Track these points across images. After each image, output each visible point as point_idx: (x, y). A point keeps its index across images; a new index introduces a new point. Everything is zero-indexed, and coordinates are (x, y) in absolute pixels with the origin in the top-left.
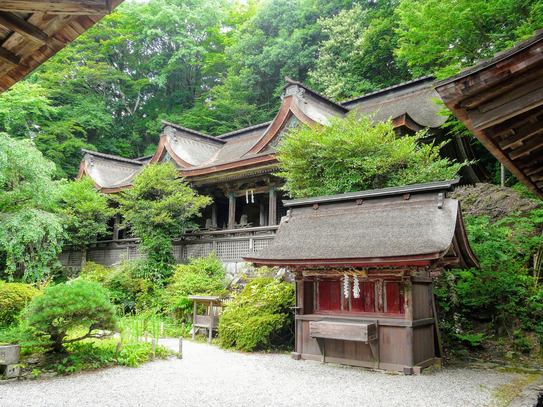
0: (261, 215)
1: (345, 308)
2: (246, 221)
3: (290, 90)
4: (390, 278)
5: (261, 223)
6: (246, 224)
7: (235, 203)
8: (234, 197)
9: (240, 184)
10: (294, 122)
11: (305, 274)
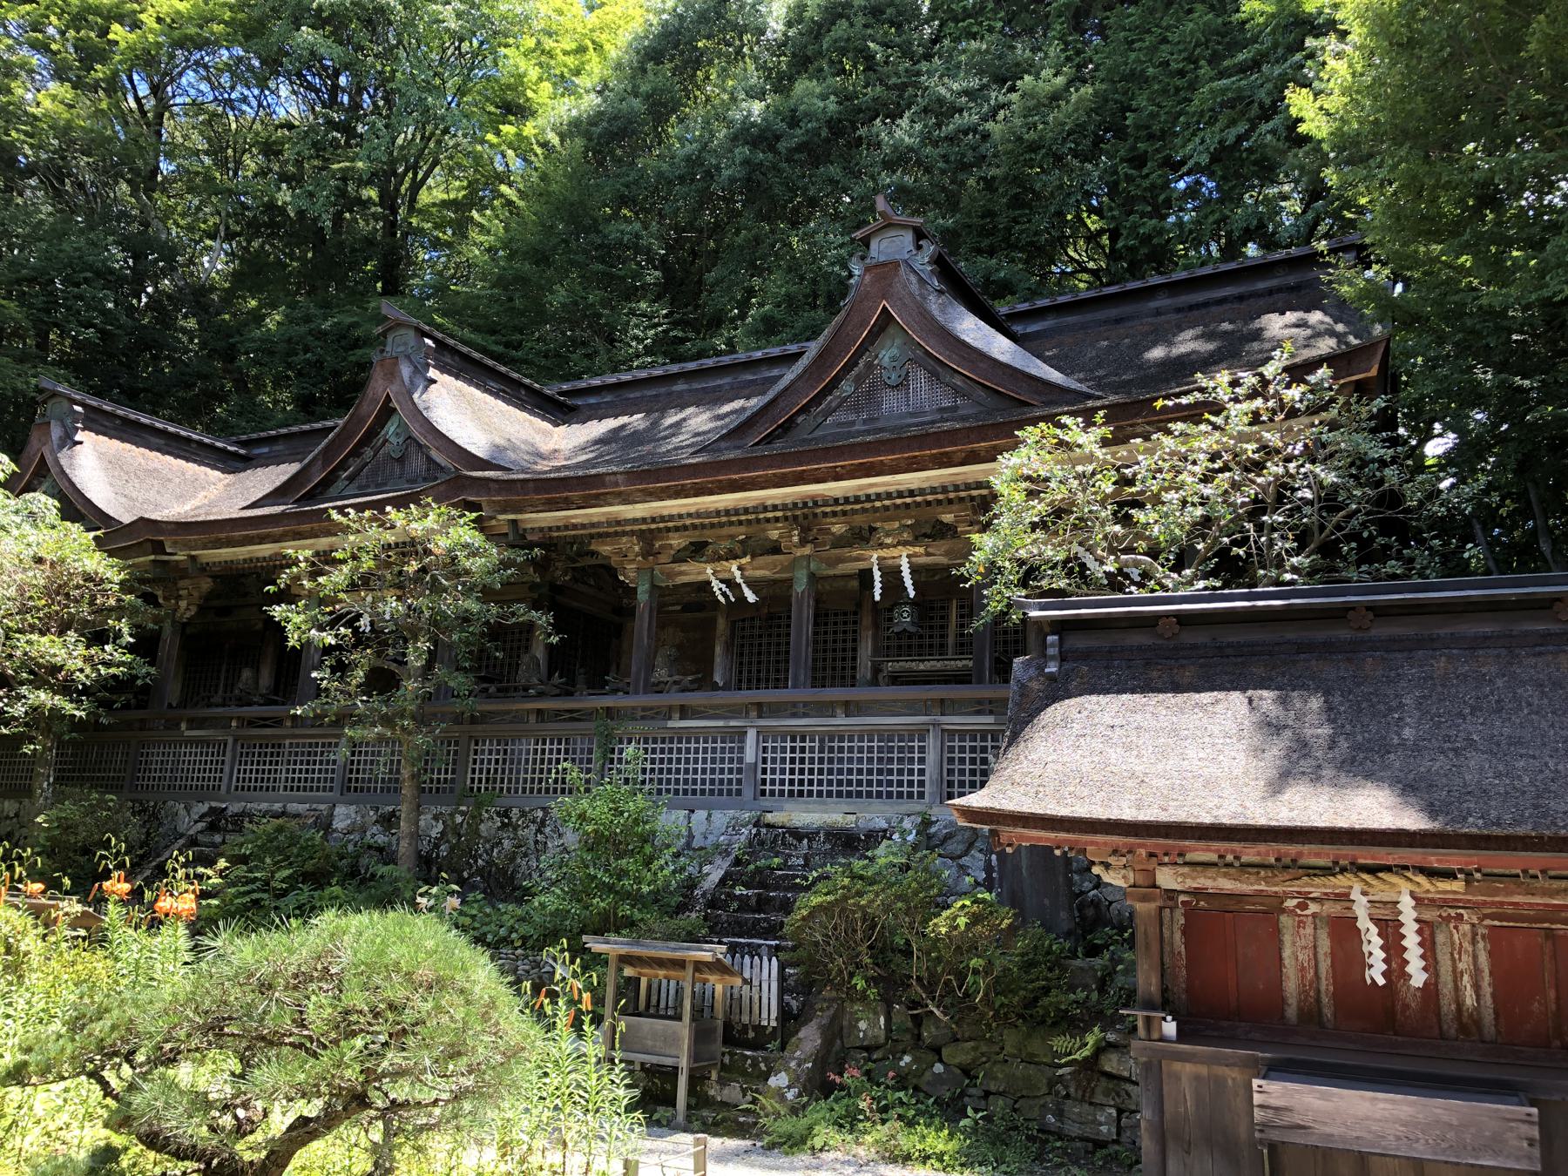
0: (718, 650)
3: (885, 243)
4: (1509, 910)
6: (676, 678)
8: (654, 587)
9: (677, 541)
10: (894, 351)
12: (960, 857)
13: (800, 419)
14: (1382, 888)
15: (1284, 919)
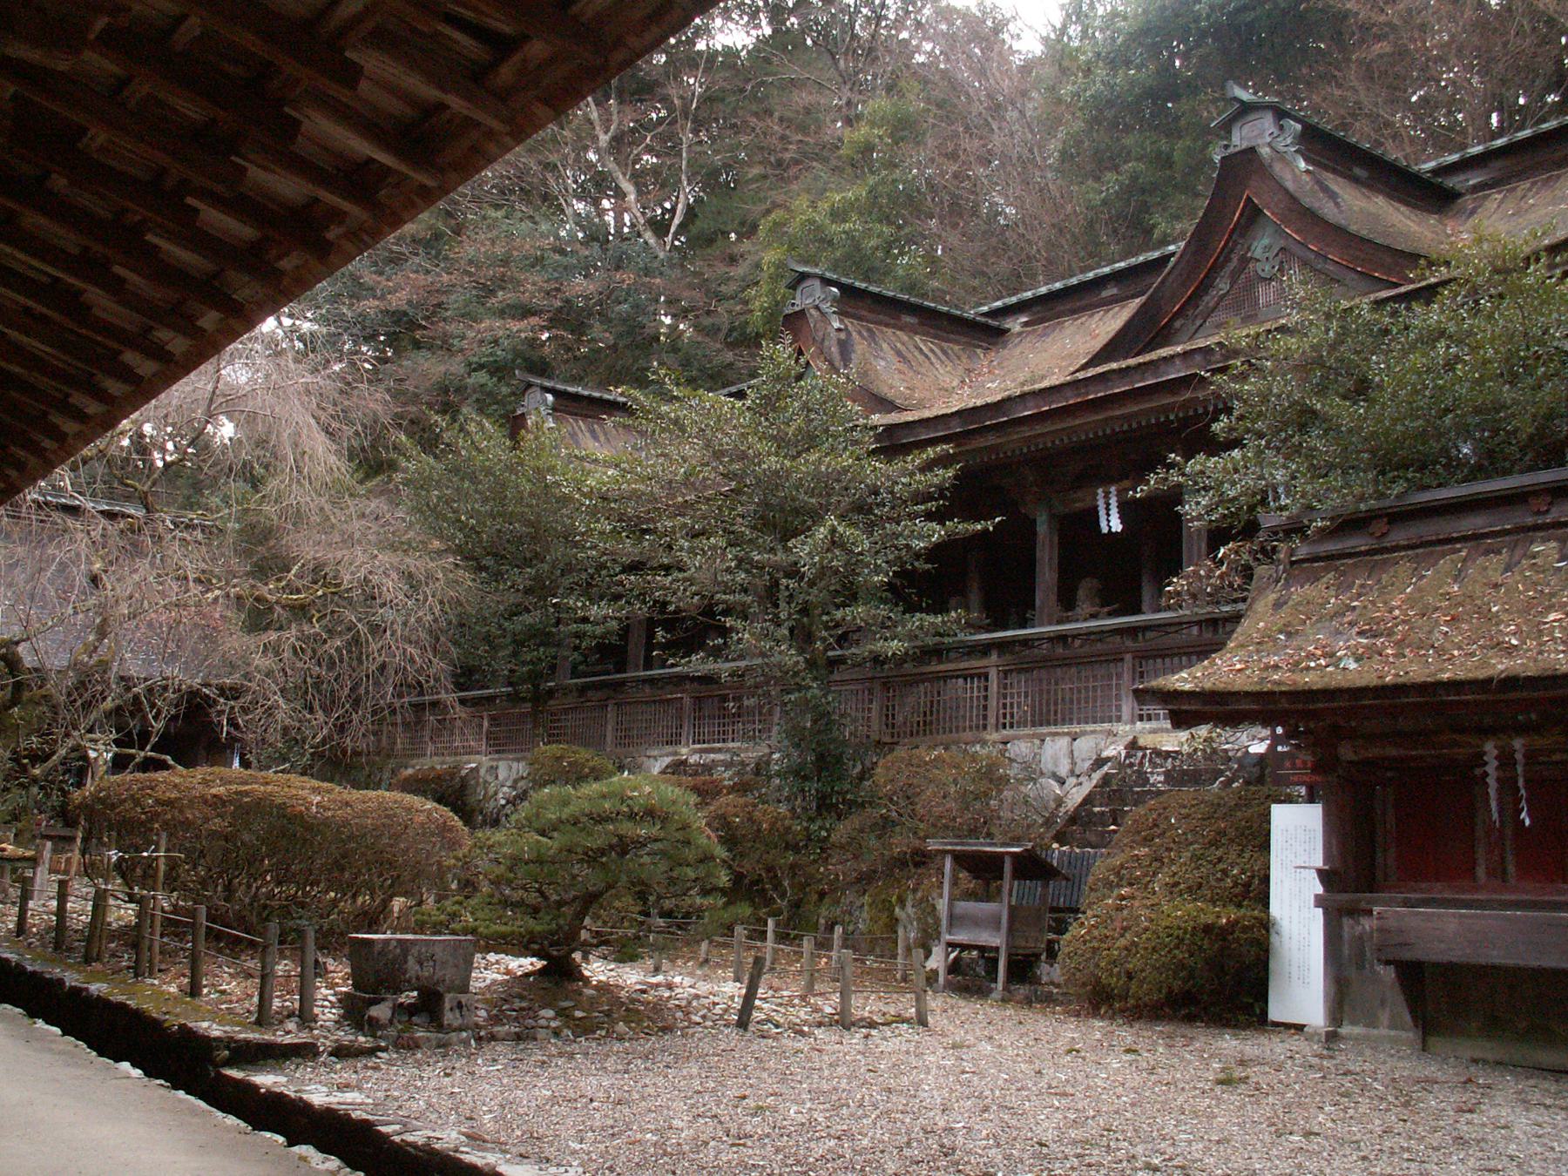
0: (1145, 579)
1: (1490, 873)
2: (1097, 600)
3: (1246, 129)
5: (1144, 608)
7: (1056, 539)
8: (1052, 516)
10: (1266, 241)
11: (1346, 752)
13: (1177, 324)
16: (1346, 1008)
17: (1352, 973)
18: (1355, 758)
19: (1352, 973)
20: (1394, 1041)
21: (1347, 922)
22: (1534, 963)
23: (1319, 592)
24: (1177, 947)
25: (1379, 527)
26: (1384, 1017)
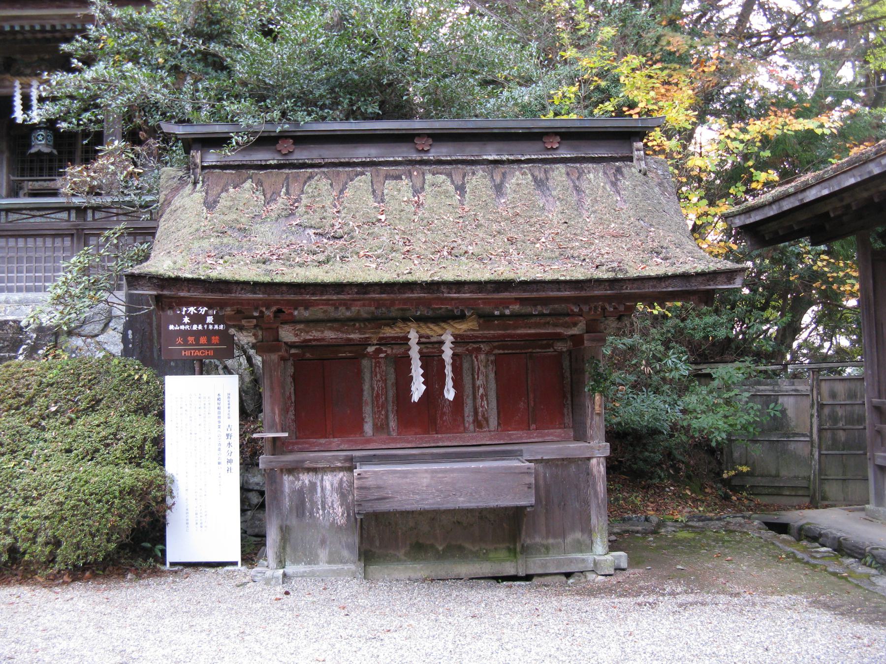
12: (97, 336)
14: (432, 331)
15: (365, 363)
16: (288, 549)
17: (293, 522)
18: (296, 339)
19: (293, 522)
20: (338, 574)
21: (287, 479)
22: (493, 504)
23: (245, 195)
24: (109, 510)
25: (286, 146)
26: (323, 554)
